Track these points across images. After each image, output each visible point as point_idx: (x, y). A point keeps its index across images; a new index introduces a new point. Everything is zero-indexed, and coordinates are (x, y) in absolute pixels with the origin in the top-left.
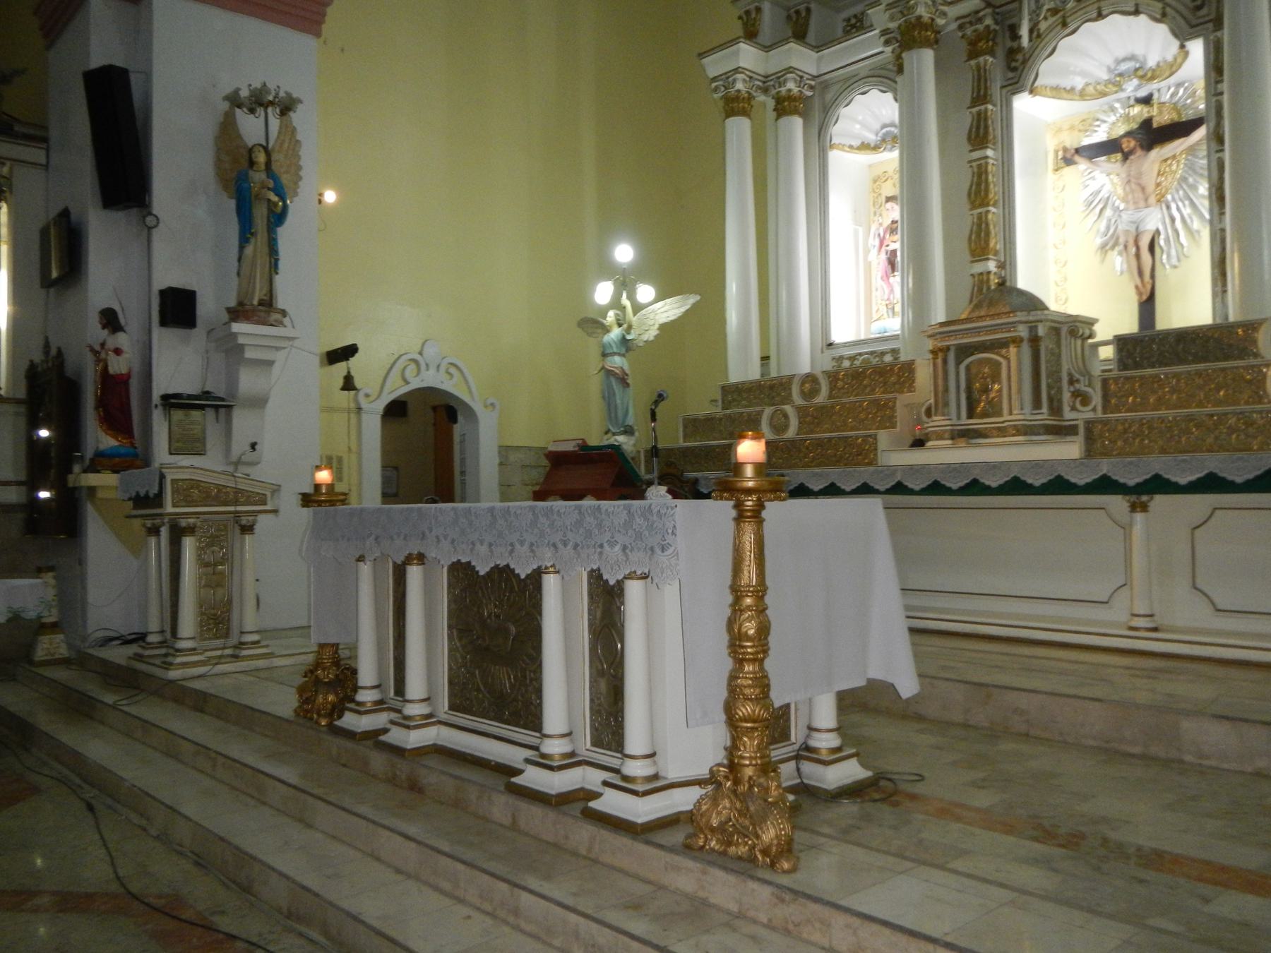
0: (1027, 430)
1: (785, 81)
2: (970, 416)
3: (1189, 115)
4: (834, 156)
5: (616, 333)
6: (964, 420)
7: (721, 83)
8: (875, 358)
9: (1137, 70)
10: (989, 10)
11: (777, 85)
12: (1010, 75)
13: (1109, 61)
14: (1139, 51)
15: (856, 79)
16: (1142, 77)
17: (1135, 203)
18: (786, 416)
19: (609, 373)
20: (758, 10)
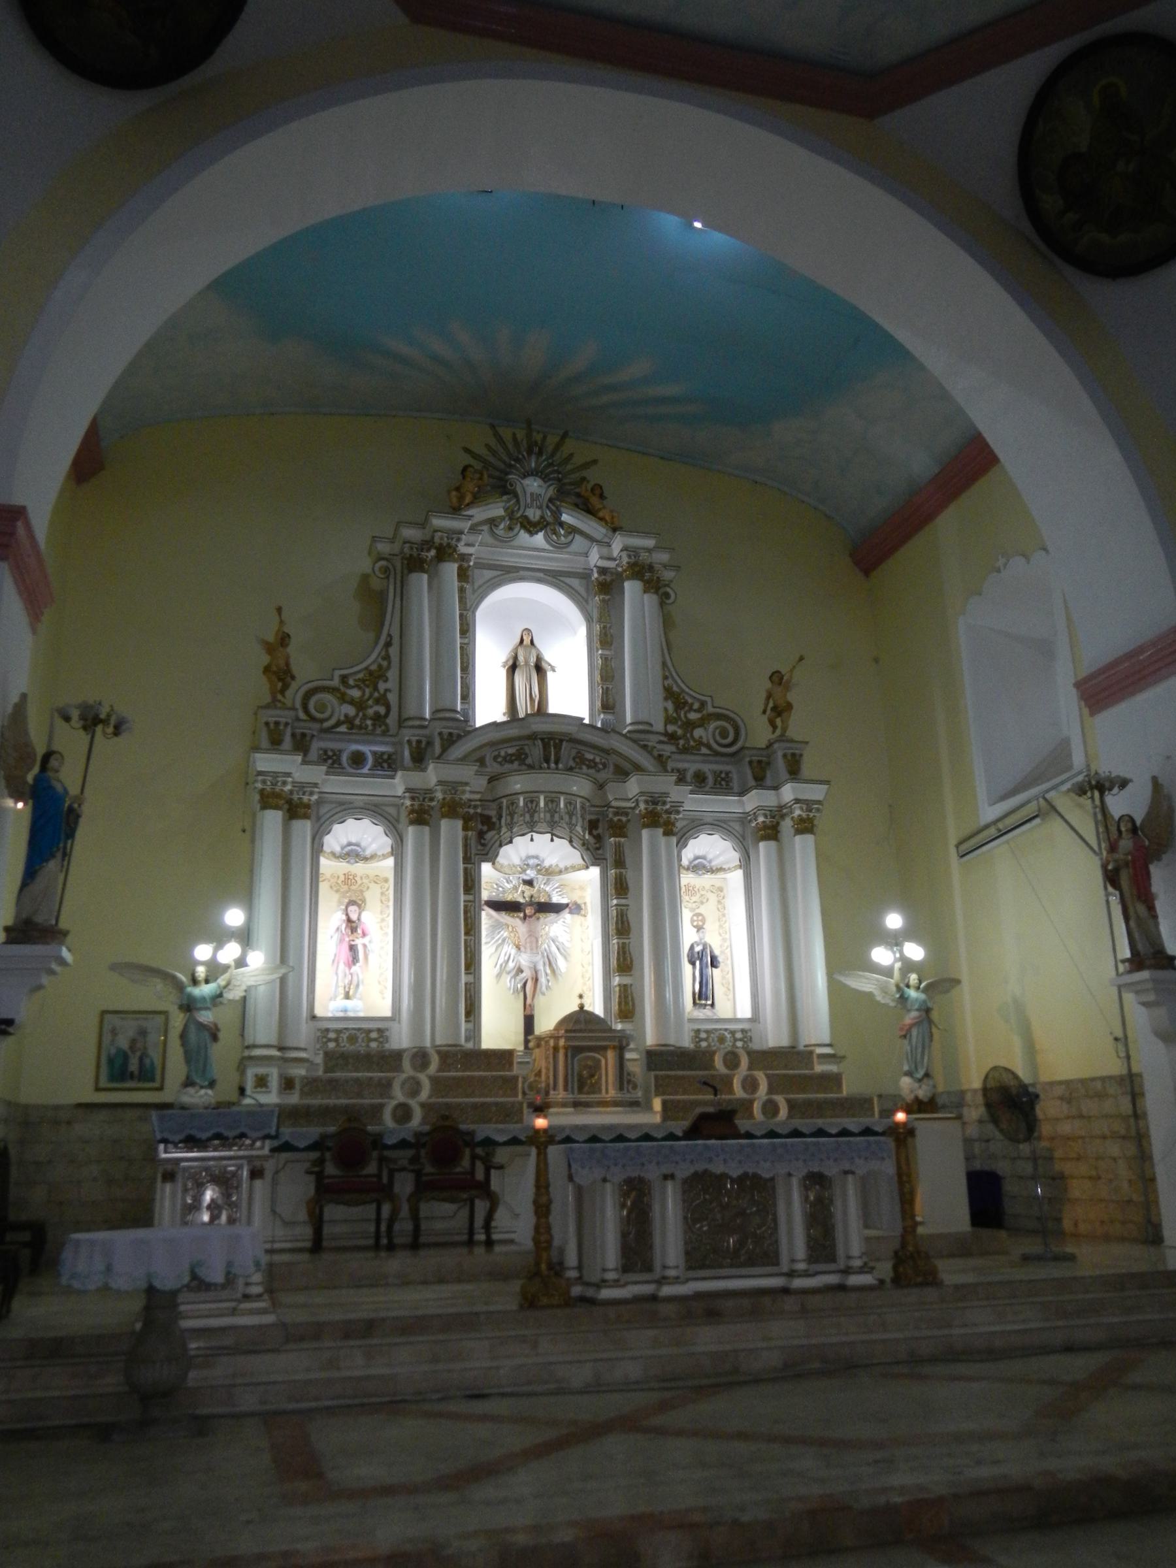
0: (616, 1103)
1: (312, 793)
2: (580, 1090)
3: (556, 899)
4: (323, 861)
5: (206, 990)
7: (269, 778)
8: (361, 1034)
9: (538, 865)
10: (478, 803)
11: (301, 793)
12: (480, 847)
13: (524, 855)
14: (542, 855)
16: (539, 872)
17: (531, 949)
19: (201, 1026)
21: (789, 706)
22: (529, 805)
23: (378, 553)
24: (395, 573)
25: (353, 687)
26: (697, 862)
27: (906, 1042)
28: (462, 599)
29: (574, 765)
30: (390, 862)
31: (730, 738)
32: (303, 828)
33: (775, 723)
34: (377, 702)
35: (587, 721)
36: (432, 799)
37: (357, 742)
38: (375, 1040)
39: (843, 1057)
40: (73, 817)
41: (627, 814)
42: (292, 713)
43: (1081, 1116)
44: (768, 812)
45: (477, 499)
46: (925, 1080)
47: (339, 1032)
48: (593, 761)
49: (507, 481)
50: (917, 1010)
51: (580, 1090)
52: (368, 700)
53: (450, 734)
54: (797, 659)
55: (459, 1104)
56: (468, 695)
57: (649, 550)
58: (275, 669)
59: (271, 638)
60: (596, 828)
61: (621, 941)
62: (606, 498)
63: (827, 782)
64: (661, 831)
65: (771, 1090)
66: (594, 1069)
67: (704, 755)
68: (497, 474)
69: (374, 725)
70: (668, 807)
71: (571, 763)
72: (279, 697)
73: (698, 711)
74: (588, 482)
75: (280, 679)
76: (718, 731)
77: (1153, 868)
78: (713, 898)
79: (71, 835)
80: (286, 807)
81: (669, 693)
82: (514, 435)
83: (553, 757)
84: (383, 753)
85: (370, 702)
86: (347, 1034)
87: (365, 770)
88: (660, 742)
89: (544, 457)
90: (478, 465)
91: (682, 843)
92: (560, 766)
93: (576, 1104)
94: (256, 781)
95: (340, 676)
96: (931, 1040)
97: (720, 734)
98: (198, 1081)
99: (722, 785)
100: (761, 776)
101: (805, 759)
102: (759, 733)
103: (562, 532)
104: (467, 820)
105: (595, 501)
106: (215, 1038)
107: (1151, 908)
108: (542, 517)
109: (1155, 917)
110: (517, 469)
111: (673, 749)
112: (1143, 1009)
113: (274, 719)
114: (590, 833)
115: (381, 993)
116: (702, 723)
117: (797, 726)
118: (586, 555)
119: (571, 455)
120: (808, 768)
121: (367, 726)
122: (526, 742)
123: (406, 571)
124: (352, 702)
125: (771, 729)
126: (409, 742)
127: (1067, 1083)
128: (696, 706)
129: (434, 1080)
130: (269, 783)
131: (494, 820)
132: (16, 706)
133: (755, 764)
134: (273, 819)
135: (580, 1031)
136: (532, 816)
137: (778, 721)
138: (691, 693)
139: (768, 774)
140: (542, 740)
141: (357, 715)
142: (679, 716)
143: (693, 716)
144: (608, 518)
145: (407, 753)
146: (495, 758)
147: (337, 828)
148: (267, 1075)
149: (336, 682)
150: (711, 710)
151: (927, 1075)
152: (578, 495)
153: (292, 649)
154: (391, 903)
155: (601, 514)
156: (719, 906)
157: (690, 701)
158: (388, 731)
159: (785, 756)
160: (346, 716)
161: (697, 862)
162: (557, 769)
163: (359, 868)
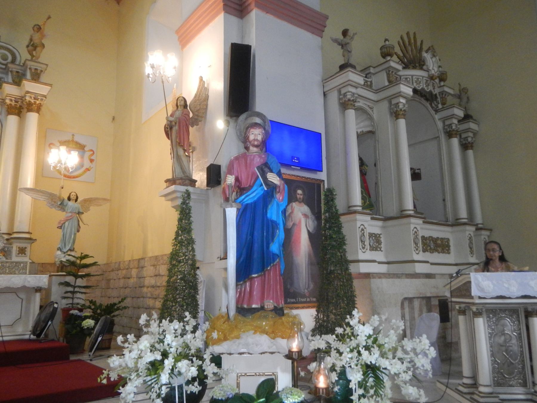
21: (43, 46)
27: (61, 230)
33: (33, 53)
39: (36, 240)
43: (160, 275)
44: (14, 99)
50: (70, 212)
54: (46, 17)
63: (51, 85)
77: (192, 130)
96: (78, 231)
117: (45, 56)
127: (156, 258)
133: (14, 74)
137: (34, 53)
159: (30, 69)
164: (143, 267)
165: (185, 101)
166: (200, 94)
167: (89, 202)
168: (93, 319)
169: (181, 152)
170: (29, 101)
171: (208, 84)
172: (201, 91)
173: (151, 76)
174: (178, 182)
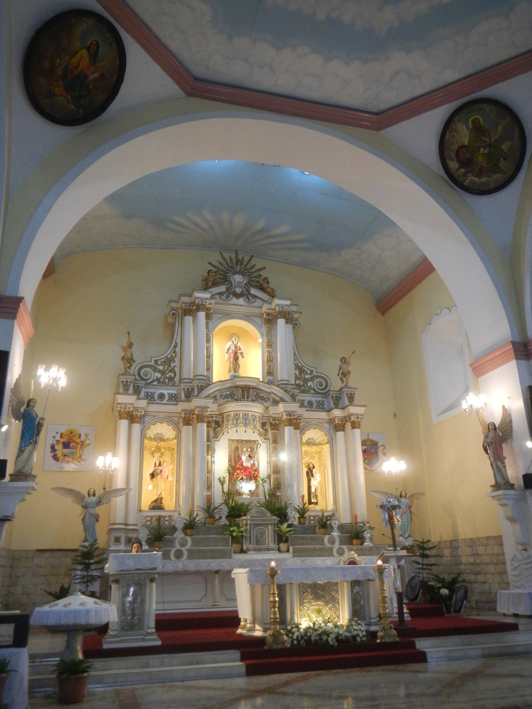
0: (273, 550)
1: (141, 412)
6: (255, 546)
7: (123, 406)
12: (214, 435)
15: (158, 417)
18: (186, 541)
20: (131, 383)
22: (236, 417)
23: (172, 307)
24: (179, 316)
25: (160, 365)
26: (309, 441)
28: (207, 327)
29: (255, 399)
30: (176, 441)
31: (324, 386)
32: (137, 427)
34: (170, 371)
35: (261, 380)
36: (193, 414)
37: (162, 389)
38: (167, 521)
39: (374, 528)
40: (40, 425)
41: (278, 420)
42: (133, 377)
43: (478, 554)
45: (215, 284)
46: (409, 538)
47: (151, 517)
48: (263, 397)
49: (227, 277)
51: (257, 543)
52: (166, 370)
53: (202, 386)
54: (352, 352)
55: (204, 550)
56: (209, 368)
57: (287, 306)
58: (126, 358)
59: (125, 345)
60: (265, 427)
61: (276, 476)
62: (269, 283)
63: (365, 406)
64: (293, 428)
65: (342, 543)
66: (263, 533)
67: (311, 393)
68: (222, 273)
69: (168, 381)
70: (296, 417)
71: (254, 398)
72: (128, 370)
73: (310, 374)
74: (262, 276)
75: (128, 363)
76: (318, 384)
77: (504, 446)
78: (317, 456)
79: (38, 434)
80: (130, 418)
81: (297, 367)
82: (230, 257)
83: (246, 397)
84: (172, 394)
85: (167, 371)
86: (155, 518)
87: (165, 402)
88: (293, 388)
89: (243, 266)
90: (214, 269)
91: (302, 433)
92: (249, 400)
93: (255, 550)
94: (117, 407)
95: (155, 360)
96: (411, 521)
97: (319, 384)
98: (89, 539)
99: (320, 407)
100: (337, 403)
101: (355, 396)
102: (336, 384)
103: (251, 298)
104: (209, 423)
105: (265, 285)
106: (97, 521)
107: (503, 463)
108: (242, 292)
109: (505, 467)
110: (232, 272)
111: (299, 391)
112: (500, 507)
113: (125, 380)
114: (262, 428)
115: (171, 499)
116: (312, 379)
117: (353, 381)
118: (261, 307)
119: (255, 265)
120: (356, 400)
121: (166, 382)
122: (234, 389)
123: (183, 315)
124: (160, 371)
125: (341, 382)
126: (184, 389)
127: (472, 540)
128: (309, 372)
129: (193, 540)
130: (123, 408)
131: (220, 423)
132: (17, 380)
134: (124, 423)
135: (257, 517)
136: (237, 421)
137: (344, 379)
138: (308, 367)
139: (340, 402)
140: (241, 388)
141: (161, 377)
142: (301, 376)
143: (307, 376)
144: (270, 292)
145: (183, 394)
146: (221, 396)
147: (153, 427)
148: (120, 537)
149: (152, 363)
150: (315, 374)
151: (409, 536)
152: (258, 282)
153: (132, 349)
154: (175, 460)
155: (268, 290)
156: (320, 460)
157: (306, 370)
158: (175, 384)
159: (347, 394)
160: (157, 377)
161: (309, 441)
162: (248, 401)
163: (162, 444)
164: (456, 548)
165: (495, 426)
166: (505, 419)
167: (412, 496)
168: (447, 588)
169: (500, 464)
170: (353, 421)
171: (510, 411)
172: (505, 416)
173: (467, 410)
174: (502, 487)
